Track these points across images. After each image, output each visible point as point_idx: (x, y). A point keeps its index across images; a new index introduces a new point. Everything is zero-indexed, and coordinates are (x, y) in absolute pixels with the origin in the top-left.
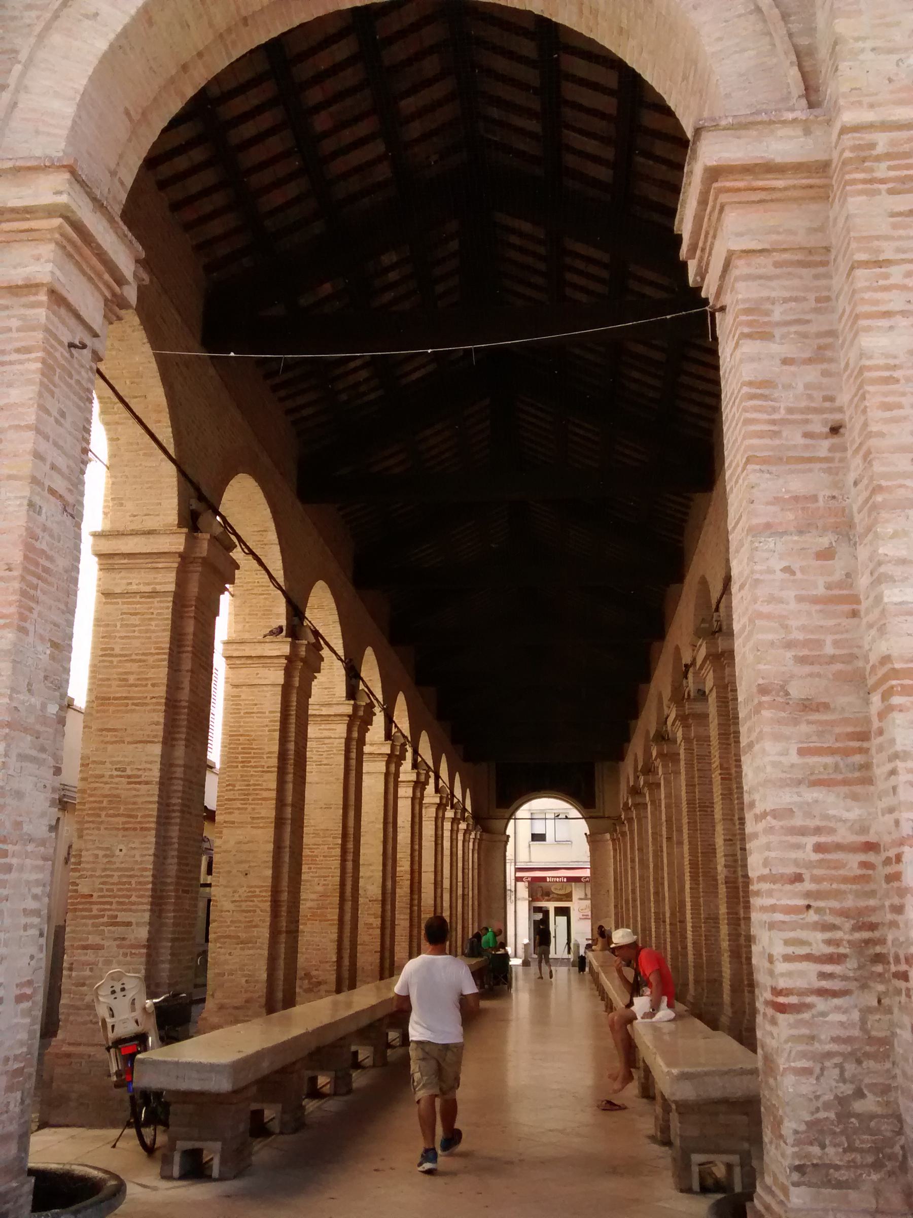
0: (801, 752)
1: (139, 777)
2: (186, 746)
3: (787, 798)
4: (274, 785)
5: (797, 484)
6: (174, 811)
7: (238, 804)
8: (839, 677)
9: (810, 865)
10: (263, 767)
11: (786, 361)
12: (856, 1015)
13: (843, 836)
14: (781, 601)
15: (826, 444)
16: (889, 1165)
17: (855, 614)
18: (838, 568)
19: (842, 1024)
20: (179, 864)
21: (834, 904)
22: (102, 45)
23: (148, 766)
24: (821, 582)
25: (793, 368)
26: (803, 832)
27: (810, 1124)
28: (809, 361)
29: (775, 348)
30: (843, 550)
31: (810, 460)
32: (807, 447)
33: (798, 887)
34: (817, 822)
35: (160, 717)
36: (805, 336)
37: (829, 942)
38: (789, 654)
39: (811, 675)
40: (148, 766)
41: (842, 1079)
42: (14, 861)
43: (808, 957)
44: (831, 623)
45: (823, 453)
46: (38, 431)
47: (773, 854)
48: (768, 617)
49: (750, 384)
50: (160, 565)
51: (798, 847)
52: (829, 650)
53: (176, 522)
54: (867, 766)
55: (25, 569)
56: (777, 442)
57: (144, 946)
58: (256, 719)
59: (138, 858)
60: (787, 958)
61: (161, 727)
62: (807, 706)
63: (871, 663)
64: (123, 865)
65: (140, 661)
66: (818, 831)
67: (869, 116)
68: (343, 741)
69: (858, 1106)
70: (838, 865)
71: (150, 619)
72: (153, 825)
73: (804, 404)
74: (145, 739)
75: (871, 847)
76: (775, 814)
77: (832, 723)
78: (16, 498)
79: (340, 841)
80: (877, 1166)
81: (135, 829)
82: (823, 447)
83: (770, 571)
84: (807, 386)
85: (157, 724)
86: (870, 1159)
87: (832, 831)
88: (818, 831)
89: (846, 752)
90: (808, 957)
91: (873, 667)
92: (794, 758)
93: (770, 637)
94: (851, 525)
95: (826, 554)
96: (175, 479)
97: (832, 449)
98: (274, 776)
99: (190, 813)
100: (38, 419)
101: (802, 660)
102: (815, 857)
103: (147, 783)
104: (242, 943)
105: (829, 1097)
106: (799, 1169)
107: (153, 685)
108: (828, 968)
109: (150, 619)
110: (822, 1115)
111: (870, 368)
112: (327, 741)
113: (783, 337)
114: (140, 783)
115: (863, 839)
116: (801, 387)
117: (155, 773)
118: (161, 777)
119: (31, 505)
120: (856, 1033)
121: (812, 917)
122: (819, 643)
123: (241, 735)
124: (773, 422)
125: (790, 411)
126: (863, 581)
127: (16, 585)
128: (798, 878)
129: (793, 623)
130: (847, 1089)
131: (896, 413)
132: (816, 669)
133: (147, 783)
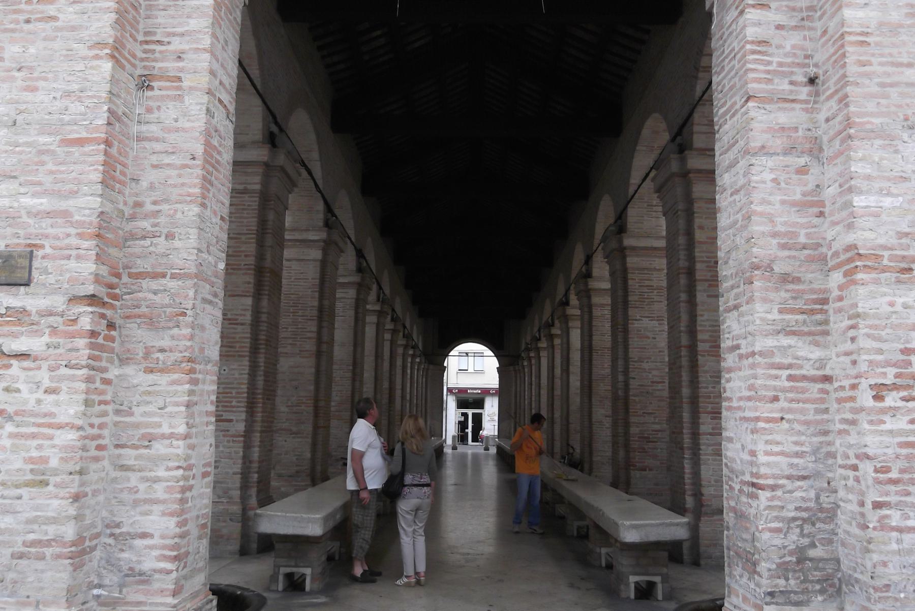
0: (781, 311)
1: (236, 320)
2: (269, 299)
3: (770, 342)
4: (314, 329)
5: (783, 118)
6: (261, 344)
7: (290, 341)
8: (811, 260)
9: (784, 390)
10: (307, 316)
11: (779, 27)
12: (812, 494)
14: (769, 203)
16: (831, 590)
17: (821, 214)
18: (811, 180)
19: (803, 499)
20: (265, 381)
21: (799, 417)
23: (243, 312)
24: (799, 190)
25: (783, 33)
26: (780, 367)
27: (779, 565)
28: (795, 28)
30: (815, 170)
31: (793, 101)
32: (791, 92)
33: (776, 405)
34: (789, 360)
35: (250, 279)
36: (794, 9)
37: (796, 443)
38: (774, 242)
39: (789, 257)
40: (243, 312)
41: (802, 535)
42: (200, 376)
43: (782, 453)
44: (804, 220)
45: (803, 97)
46: (212, 54)
47: (759, 382)
48: (761, 214)
49: (752, 42)
50: (250, 170)
51: (777, 377)
52: (802, 239)
53: (261, 140)
54: (826, 322)
55: (206, 161)
56: (770, 87)
57: (242, 436)
58: (302, 284)
59: (237, 376)
60: (767, 453)
61: (251, 286)
62: (786, 279)
63: (833, 250)
64: (226, 381)
65: (235, 238)
66: (790, 366)
68: (354, 300)
69: (812, 553)
70: (804, 391)
71: (243, 209)
72: (247, 354)
73: (789, 60)
74: (240, 293)
75: (827, 379)
76: (761, 354)
77: (803, 292)
78: (197, 104)
79: (351, 368)
80: (822, 592)
81: (234, 356)
82: (804, 92)
83: (764, 182)
84: (793, 47)
85: (249, 283)
86: (818, 587)
87: (801, 367)
88: (790, 366)
89: (812, 312)
90: (782, 453)
91: (836, 254)
92: (775, 315)
93: (761, 228)
94: (821, 150)
95: (802, 171)
96: (260, 109)
97: (809, 95)
98: (315, 323)
99: (271, 346)
100: (212, 44)
101: (784, 247)
102: (787, 384)
103: (242, 324)
104: (293, 434)
105: (793, 547)
106: (771, 594)
107: (246, 256)
108: (796, 461)
109: (243, 209)
110: (788, 559)
111: (850, 33)
112: (342, 300)
113: (777, 9)
114: (237, 324)
115: (821, 373)
116: (788, 48)
117: (248, 318)
118: (252, 321)
119: (208, 110)
120: (812, 504)
121: (785, 425)
122: (795, 235)
123: (292, 294)
124: (768, 72)
125: (780, 64)
126: (830, 192)
127: (199, 172)
128: (776, 399)
129: (779, 220)
130: (806, 541)
131: (867, 68)
132: (793, 253)
133: (242, 324)
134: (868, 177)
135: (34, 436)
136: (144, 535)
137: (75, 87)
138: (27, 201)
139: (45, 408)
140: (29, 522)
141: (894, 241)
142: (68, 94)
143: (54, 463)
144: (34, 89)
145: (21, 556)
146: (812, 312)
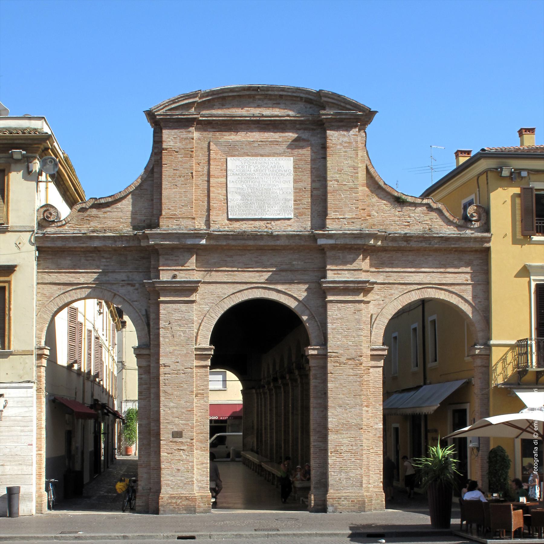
3: (316, 444)
11: (319, 383)
13: (322, 448)
15: (323, 395)
22: (215, 323)
26: (317, 448)
29: (317, 381)
62: (319, 432)
67: (332, 351)
88: (319, 448)
95: (322, 411)
128: (316, 454)
134: (331, 415)
135: (186, 464)
136: (203, 481)
137: (188, 400)
138: (181, 422)
139: (188, 459)
140: (188, 478)
141: (335, 426)
142: (187, 402)
143: (190, 468)
144: (180, 401)
145: (185, 484)
146: (323, 438)
